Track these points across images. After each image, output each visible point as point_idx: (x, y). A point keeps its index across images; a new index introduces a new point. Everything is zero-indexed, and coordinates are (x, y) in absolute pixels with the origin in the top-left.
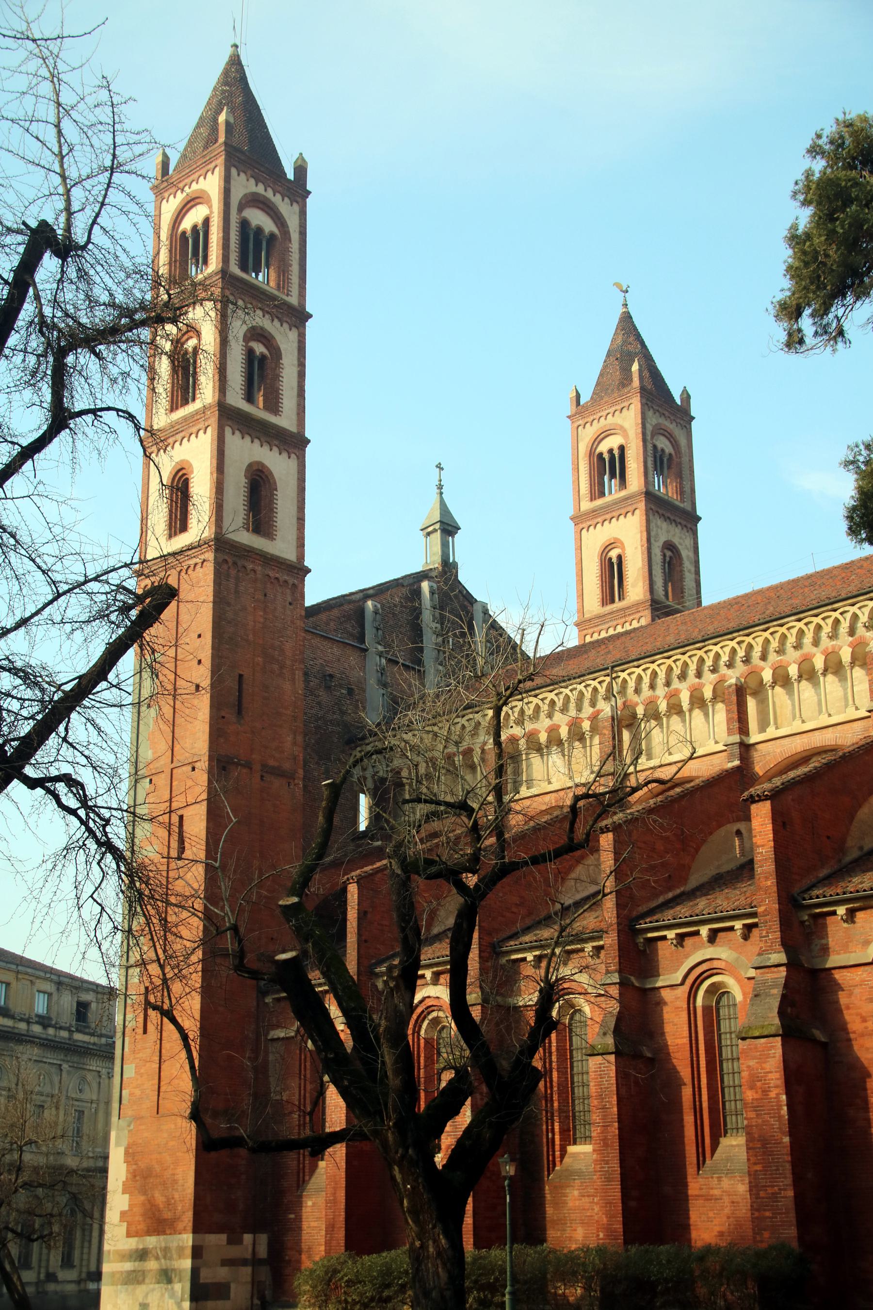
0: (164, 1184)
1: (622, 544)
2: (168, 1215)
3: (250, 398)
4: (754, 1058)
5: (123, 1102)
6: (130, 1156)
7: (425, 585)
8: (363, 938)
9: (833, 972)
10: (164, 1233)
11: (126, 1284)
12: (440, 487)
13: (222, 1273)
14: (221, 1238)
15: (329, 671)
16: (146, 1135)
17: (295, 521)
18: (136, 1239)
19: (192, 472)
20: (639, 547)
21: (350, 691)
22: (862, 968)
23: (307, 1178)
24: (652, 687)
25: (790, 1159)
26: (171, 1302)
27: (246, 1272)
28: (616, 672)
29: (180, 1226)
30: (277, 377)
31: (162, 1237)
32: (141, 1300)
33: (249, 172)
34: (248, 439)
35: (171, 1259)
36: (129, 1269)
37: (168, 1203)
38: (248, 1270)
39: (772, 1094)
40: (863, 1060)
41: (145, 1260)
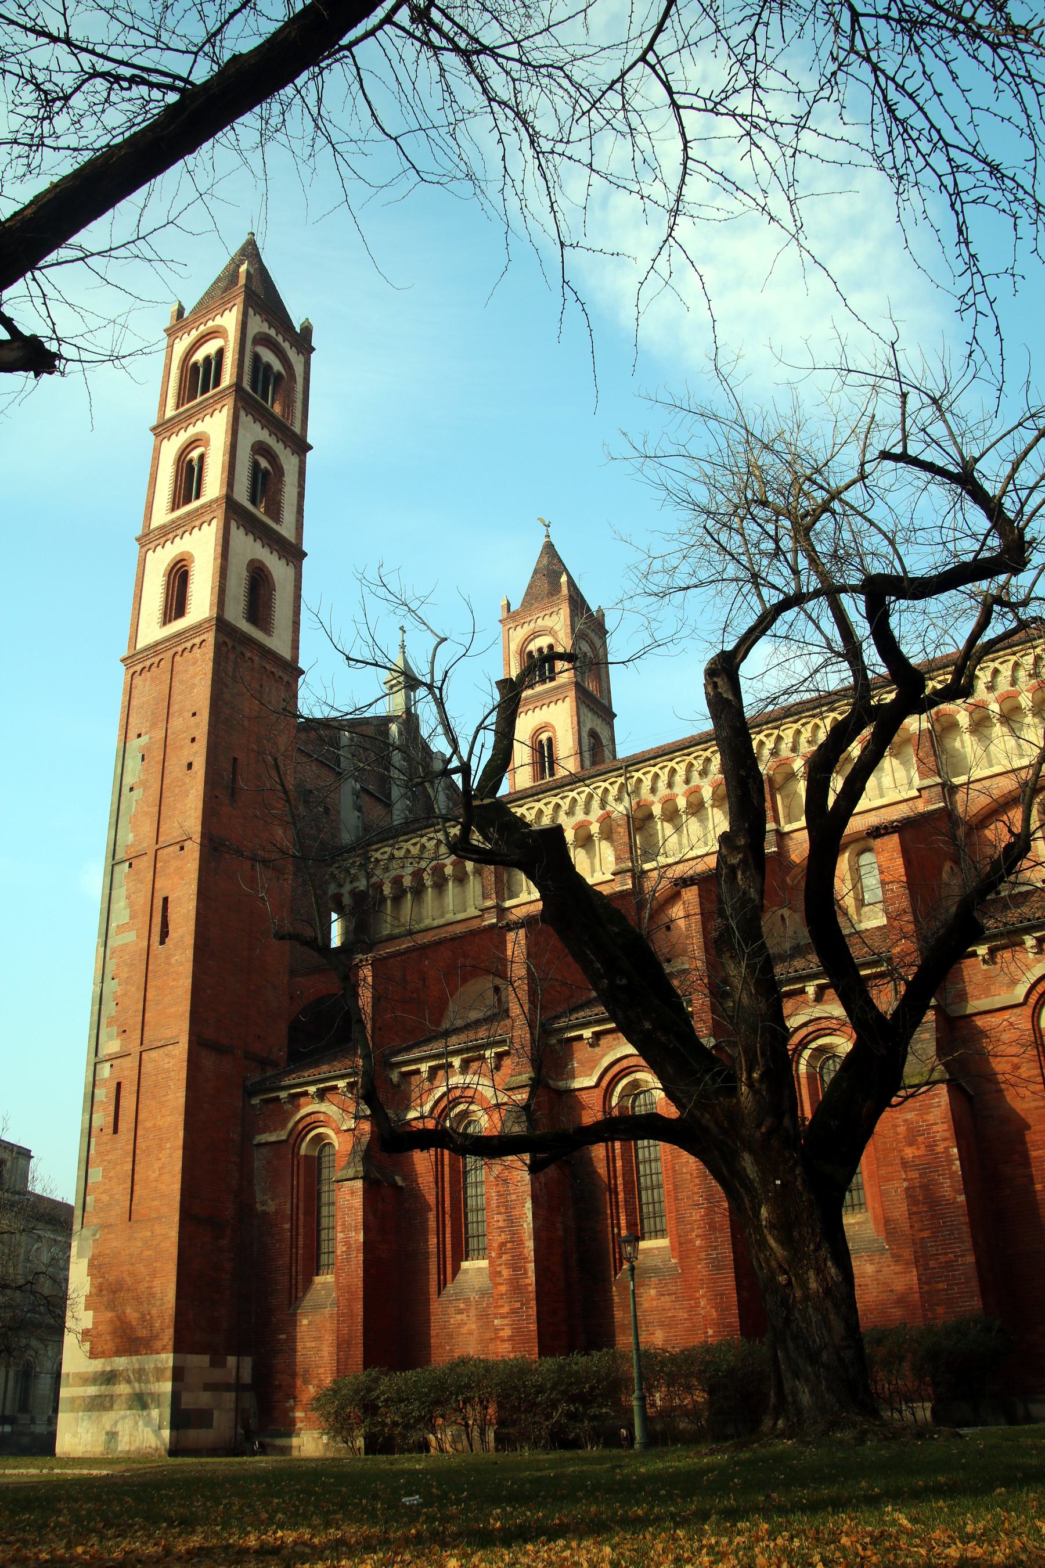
0: (137, 1298)
1: (553, 727)
2: (143, 1333)
3: (253, 500)
4: (912, 1110)
5: (87, 1209)
6: (95, 1268)
7: (394, 728)
8: (378, 1025)
9: (974, 1018)
10: (137, 1353)
11: (89, 1410)
12: (403, 647)
13: (205, 1399)
14: (204, 1360)
15: (308, 787)
16: (114, 1244)
17: (290, 623)
18: (103, 1360)
19: (193, 562)
20: (570, 730)
21: (327, 811)
22: (1010, 1011)
23: (300, 1294)
24: (670, 785)
25: (967, 1220)
26: (148, 1430)
27: (230, 1397)
28: (630, 772)
29: (159, 1345)
30: (279, 491)
31: (134, 1358)
32: (108, 1428)
33: (264, 316)
34: (251, 537)
35: (147, 1382)
36: (94, 1394)
37: (142, 1319)
38: (232, 1395)
39: (940, 1149)
40: (1018, 1110)
41: (114, 1384)
